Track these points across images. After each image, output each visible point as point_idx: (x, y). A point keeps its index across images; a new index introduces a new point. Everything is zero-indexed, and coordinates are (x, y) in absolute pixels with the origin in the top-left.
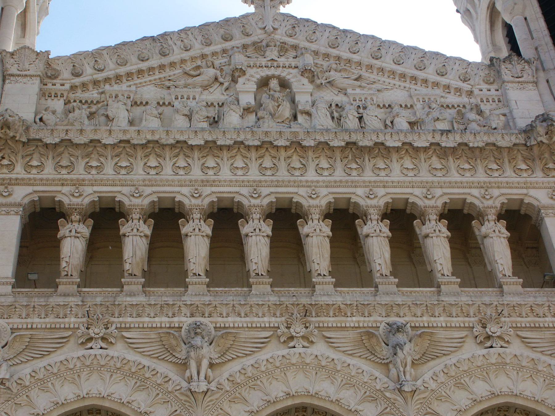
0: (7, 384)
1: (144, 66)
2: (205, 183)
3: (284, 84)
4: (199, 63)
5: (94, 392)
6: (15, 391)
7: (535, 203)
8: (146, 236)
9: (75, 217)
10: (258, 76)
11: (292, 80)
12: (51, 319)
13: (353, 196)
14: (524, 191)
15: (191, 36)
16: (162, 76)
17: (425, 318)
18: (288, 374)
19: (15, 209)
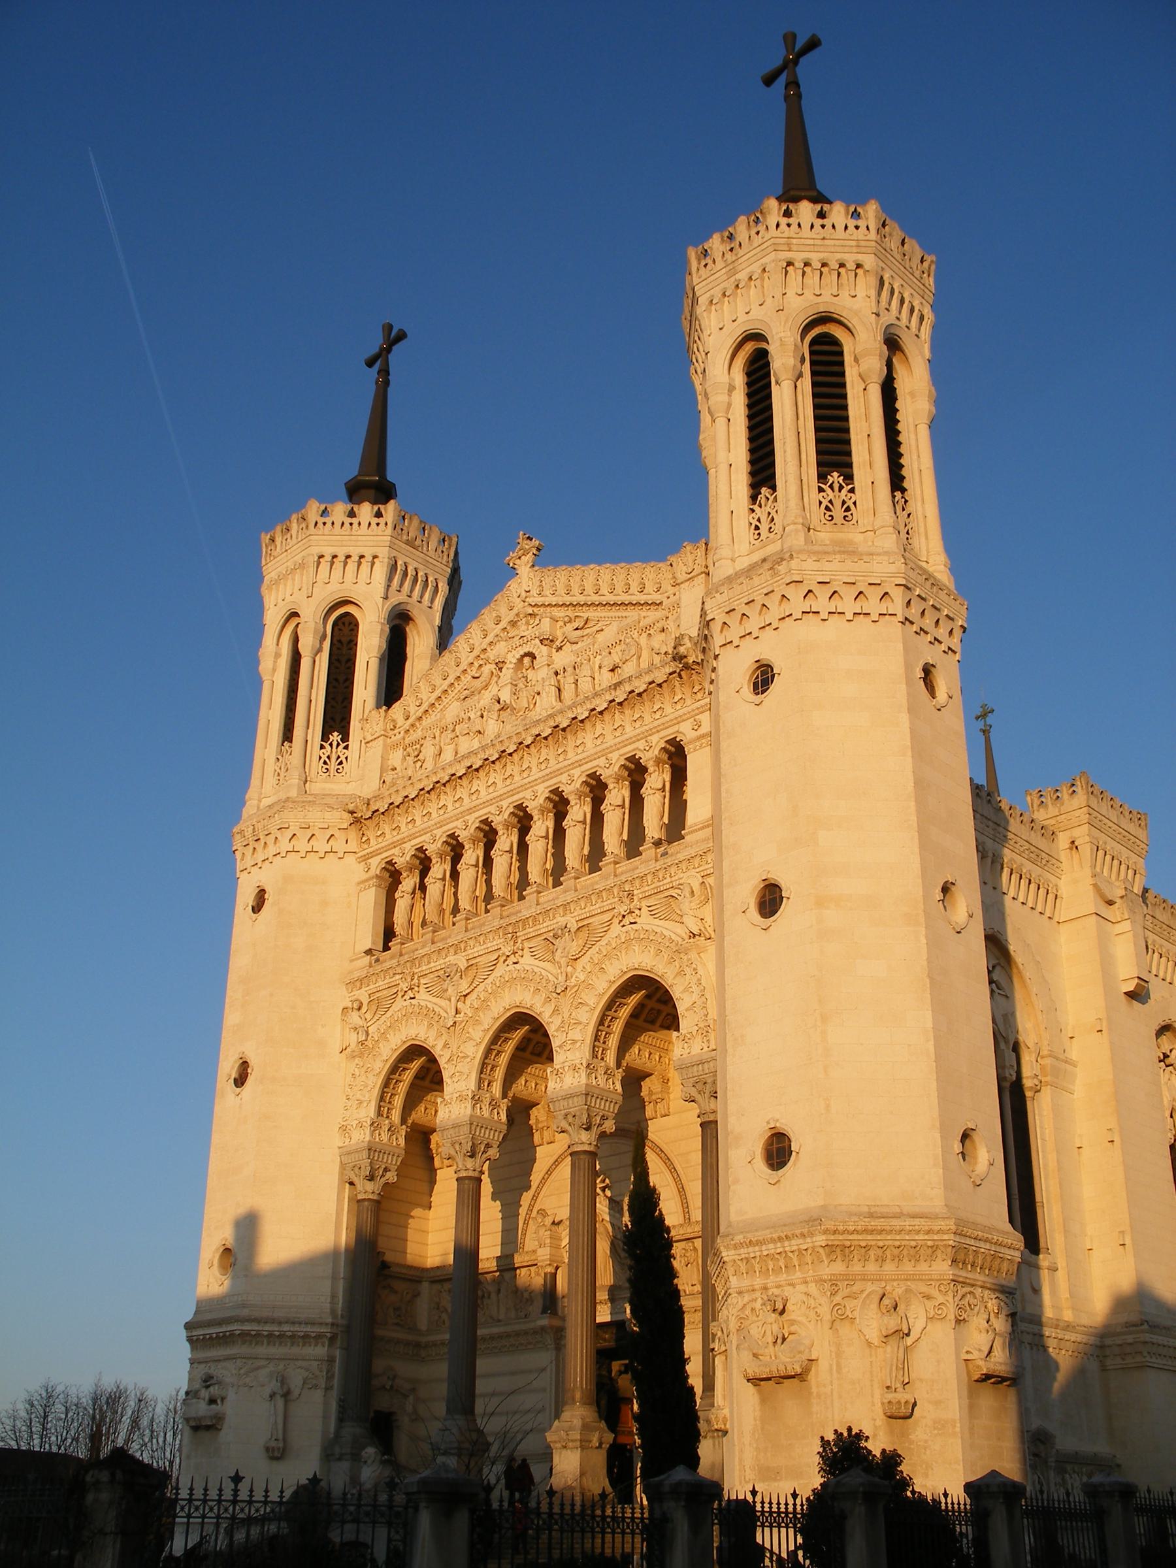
6: (371, 1046)
9: (404, 874)
10: (514, 661)
14: (675, 728)
17: (587, 910)
19: (371, 882)
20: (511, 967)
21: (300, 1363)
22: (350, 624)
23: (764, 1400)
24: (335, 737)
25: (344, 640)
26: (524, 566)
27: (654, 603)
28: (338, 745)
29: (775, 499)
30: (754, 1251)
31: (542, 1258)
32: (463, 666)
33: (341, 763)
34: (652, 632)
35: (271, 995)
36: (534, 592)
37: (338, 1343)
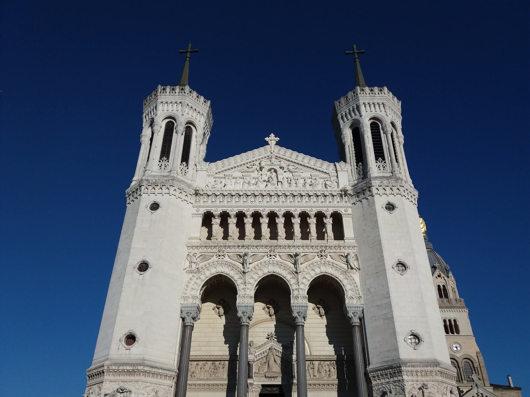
0: (199, 269)
2: (251, 207)
3: (276, 171)
5: (220, 271)
7: (341, 213)
8: (235, 224)
9: (216, 217)
11: (278, 170)
15: (249, 155)
17: (306, 250)
18: (269, 266)
19: (200, 215)
22: (189, 130)
24: (184, 163)
27: (326, 173)
29: (385, 162)
31: (251, 358)
33: (186, 173)
34: (325, 180)
35: (163, 242)
36: (276, 151)
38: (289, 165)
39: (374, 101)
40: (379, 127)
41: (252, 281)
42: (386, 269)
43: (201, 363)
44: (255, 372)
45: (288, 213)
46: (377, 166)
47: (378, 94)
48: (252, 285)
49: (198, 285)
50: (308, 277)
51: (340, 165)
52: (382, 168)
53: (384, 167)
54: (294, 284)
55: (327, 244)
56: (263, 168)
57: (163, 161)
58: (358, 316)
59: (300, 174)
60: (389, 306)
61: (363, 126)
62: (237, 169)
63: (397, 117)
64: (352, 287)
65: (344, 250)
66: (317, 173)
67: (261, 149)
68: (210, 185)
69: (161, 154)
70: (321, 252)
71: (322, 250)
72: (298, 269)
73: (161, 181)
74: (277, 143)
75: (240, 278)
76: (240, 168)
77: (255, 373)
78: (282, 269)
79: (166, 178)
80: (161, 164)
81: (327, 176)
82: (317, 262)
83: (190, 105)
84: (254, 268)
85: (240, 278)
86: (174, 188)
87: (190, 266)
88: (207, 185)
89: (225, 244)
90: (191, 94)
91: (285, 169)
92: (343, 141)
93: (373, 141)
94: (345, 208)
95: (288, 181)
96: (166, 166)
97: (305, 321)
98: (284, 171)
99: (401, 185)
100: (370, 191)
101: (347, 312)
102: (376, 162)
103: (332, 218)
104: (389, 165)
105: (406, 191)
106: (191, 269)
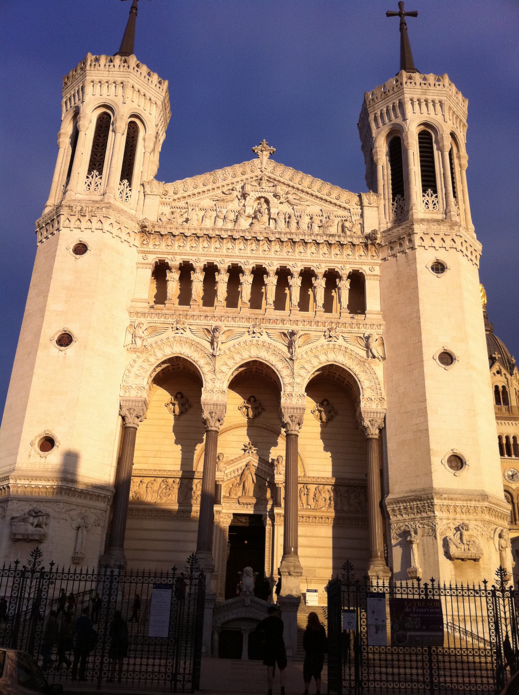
1: (205, 189)
2: (227, 256)
3: (267, 201)
4: (230, 187)
7: (364, 273)
9: (173, 270)
12: (162, 319)
13: (288, 266)
14: (360, 266)
16: (213, 194)
17: (307, 327)
19: (149, 266)
20: (257, 339)
21: (92, 510)
22: (134, 128)
23: (456, 567)
24: (125, 181)
25: (131, 135)
26: (265, 156)
28: (127, 188)
29: (436, 197)
30: (450, 502)
32: (219, 184)
33: (127, 197)
34: (343, 219)
36: (270, 169)
37: (110, 503)
38: (287, 193)
39: (427, 97)
40: (431, 139)
41: (224, 369)
42: (423, 361)
43: (146, 480)
44: (225, 496)
45: (284, 269)
46: (425, 203)
47: (435, 85)
48: (225, 374)
49: (145, 370)
50: (307, 366)
51: (368, 198)
52: (431, 205)
53: (435, 204)
54: (287, 376)
55: (339, 320)
56: (247, 195)
57: (92, 177)
58: (376, 425)
59: (304, 208)
60: (423, 413)
61: (407, 136)
62: (206, 195)
63: (460, 124)
64: (371, 384)
65: (365, 330)
66: (331, 208)
67: (247, 165)
68: (164, 219)
69: (90, 166)
70: (330, 331)
71: (332, 328)
72: (294, 354)
73: (90, 208)
74: (272, 156)
75: (207, 364)
76: (211, 193)
77: (225, 497)
78: (270, 353)
79: (97, 205)
80: (89, 181)
81: (345, 213)
82: (323, 345)
83: (137, 87)
84: (229, 349)
85: (208, 363)
86: (109, 221)
87: (134, 342)
88: (160, 219)
89: (186, 312)
90: (138, 70)
91: (282, 198)
92: (375, 158)
93: (421, 161)
94: (370, 266)
95: (285, 219)
96: (97, 186)
97: (300, 428)
98: (279, 201)
99: (458, 234)
100: (410, 241)
101: (362, 419)
102: (424, 196)
103: (349, 280)
104: (443, 201)
105: (464, 243)
106: (135, 346)
